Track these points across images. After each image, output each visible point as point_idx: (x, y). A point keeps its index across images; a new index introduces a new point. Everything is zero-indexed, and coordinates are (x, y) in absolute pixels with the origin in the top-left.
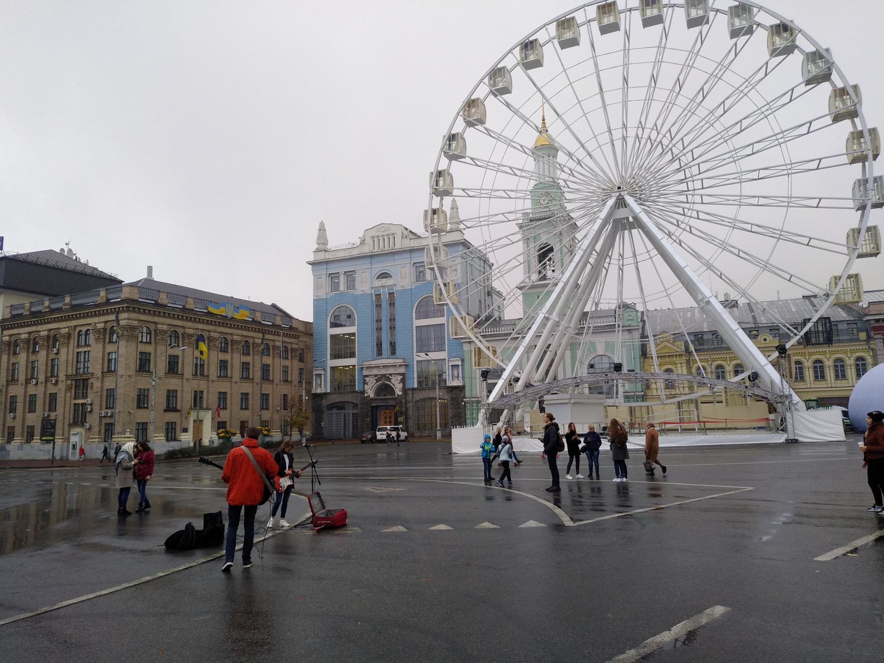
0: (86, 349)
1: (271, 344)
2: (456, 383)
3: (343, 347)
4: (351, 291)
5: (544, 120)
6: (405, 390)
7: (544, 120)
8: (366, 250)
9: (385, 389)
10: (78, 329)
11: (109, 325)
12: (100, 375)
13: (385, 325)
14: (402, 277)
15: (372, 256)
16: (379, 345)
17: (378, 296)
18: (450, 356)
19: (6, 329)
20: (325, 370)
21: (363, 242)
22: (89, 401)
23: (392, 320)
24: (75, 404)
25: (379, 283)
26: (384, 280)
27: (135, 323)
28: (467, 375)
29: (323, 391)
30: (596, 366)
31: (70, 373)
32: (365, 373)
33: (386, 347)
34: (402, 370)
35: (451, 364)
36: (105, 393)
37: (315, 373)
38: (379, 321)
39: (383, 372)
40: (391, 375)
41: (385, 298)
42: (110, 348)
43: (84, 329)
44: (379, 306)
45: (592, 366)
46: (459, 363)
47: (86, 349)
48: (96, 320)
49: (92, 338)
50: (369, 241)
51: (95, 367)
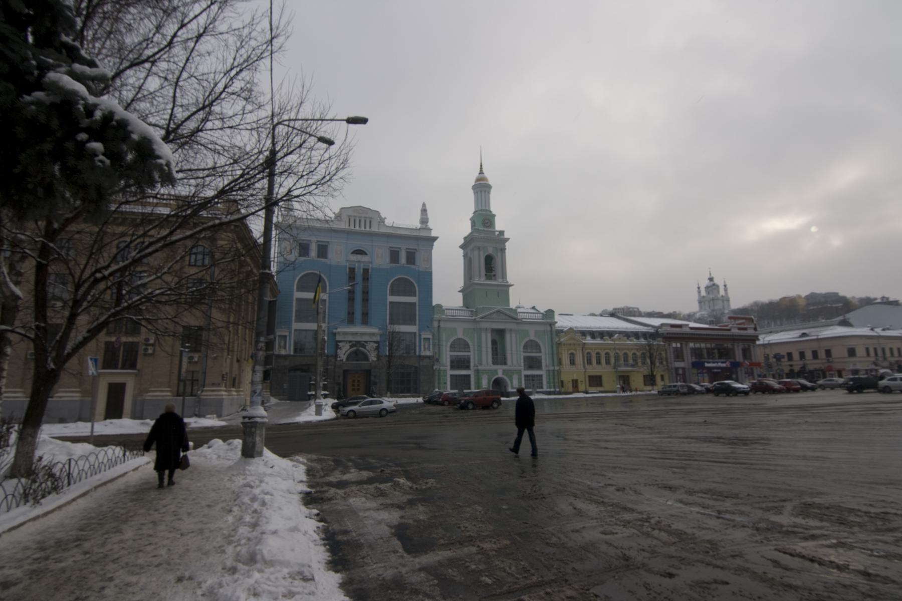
2: (428, 353)
4: (323, 260)
5: (481, 168)
6: (378, 357)
7: (481, 168)
8: (343, 225)
9: (358, 354)
13: (359, 296)
14: (379, 258)
15: (348, 233)
16: (351, 314)
17: (352, 270)
20: (290, 333)
21: (338, 216)
23: (366, 293)
25: (355, 258)
26: (359, 257)
29: (288, 353)
32: (338, 338)
33: (358, 315)
34: (378, 339)
35: (423, 336)
39: (358, 339)
40: (366, 342)
41: (359, 273)
50: (345, 218)
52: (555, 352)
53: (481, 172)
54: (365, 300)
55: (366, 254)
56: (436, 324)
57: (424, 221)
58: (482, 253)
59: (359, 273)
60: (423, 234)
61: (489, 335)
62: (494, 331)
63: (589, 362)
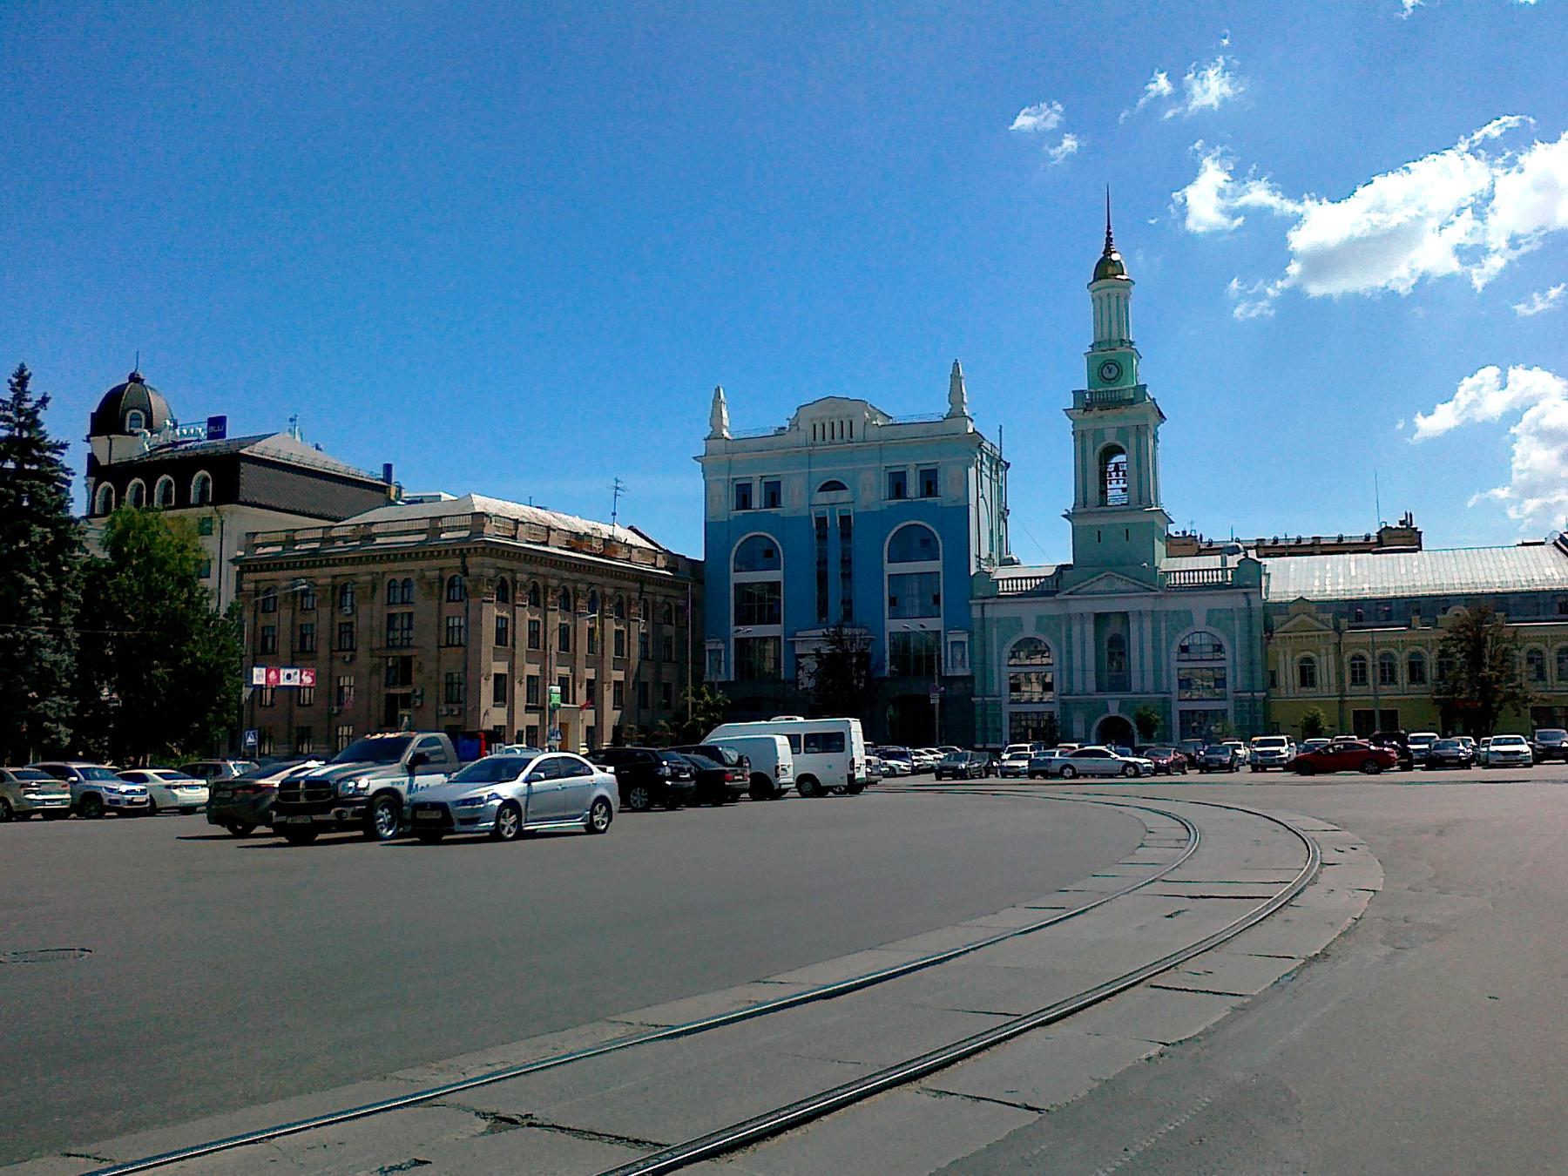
0: (405, 609)
1: (650, 598)
2: (960, 672)
3: (757, 604)
7: (1109, 233)
10: (387, 578)
11: (448, 575)
12: (434, 652)
14: (868, 493)
17: (821, 521)
18: (948, 628)
19: (249, 571)
21: (795, 423)
22: (385, 691)
23: (846, 562)
24: (388, 696)
26: (832, 495)
27: (492, 572)
28: (977, 659)
29: (722, 679)
30: (1192, 650)
31: (376, 645)
35: (949, 639)
36: (443, 678)
37: (708, 647)
38: (822, 562)
41: (834, 525)
42: (450, 609)
43: (400, 578)
44: (822, 535)
45: (1184, 649)
46: (965, 638)
47: (405, 609)
48: (424, 564)
49: (417, 592)
50: (806, 426)
51: (425, 638)
52: (1258, 656)
53: (1108, 251)
54: (847, 577)
55: (843, 487)
56: (976, 612)
57: (955, 396)
58: (1089, 445)
59: (834, 525)
60: (953, 425)
61: (1090, 628)
62: (1101, 618)
63: (1359, 676)
